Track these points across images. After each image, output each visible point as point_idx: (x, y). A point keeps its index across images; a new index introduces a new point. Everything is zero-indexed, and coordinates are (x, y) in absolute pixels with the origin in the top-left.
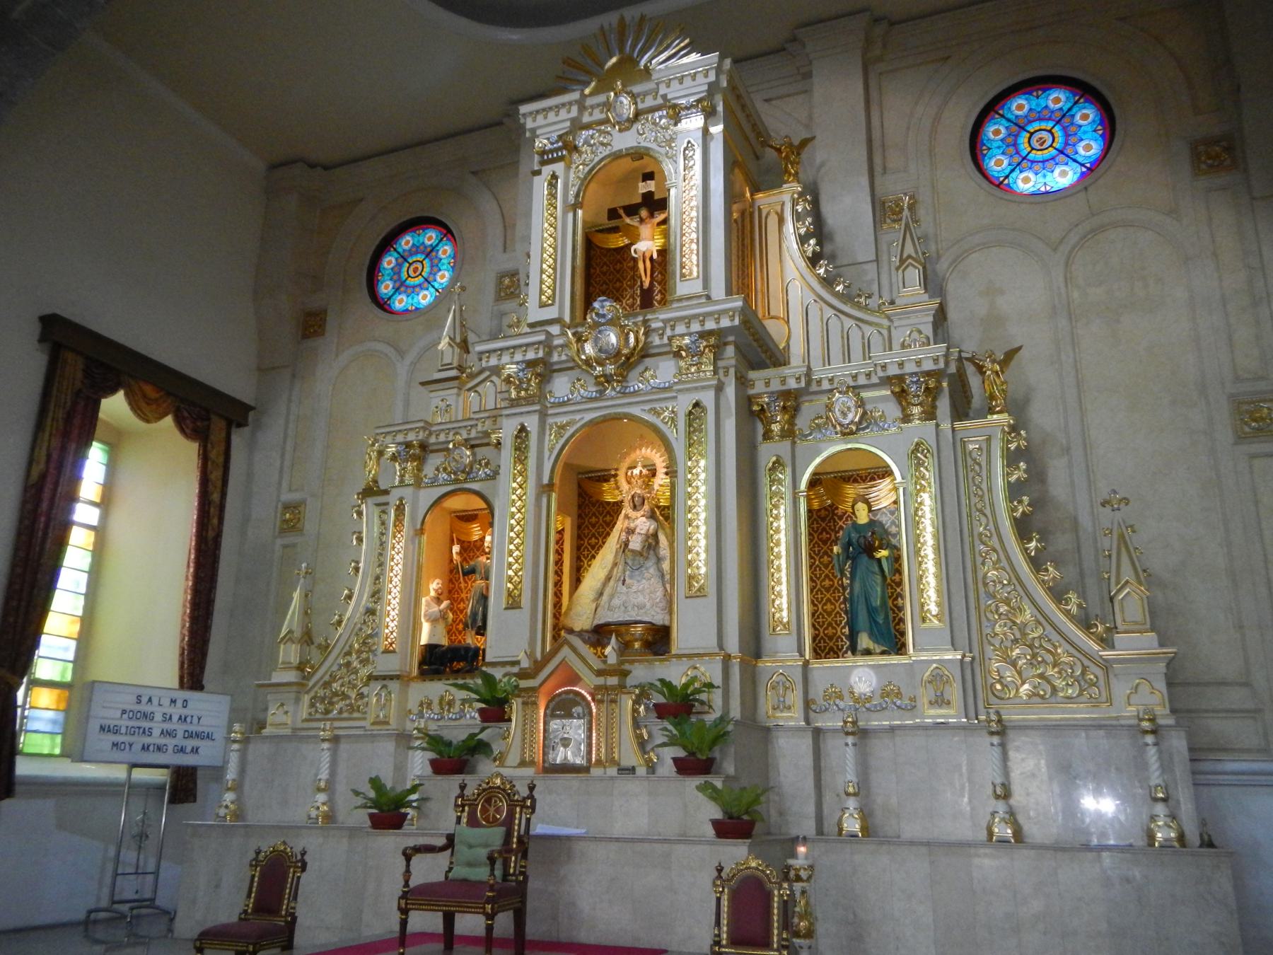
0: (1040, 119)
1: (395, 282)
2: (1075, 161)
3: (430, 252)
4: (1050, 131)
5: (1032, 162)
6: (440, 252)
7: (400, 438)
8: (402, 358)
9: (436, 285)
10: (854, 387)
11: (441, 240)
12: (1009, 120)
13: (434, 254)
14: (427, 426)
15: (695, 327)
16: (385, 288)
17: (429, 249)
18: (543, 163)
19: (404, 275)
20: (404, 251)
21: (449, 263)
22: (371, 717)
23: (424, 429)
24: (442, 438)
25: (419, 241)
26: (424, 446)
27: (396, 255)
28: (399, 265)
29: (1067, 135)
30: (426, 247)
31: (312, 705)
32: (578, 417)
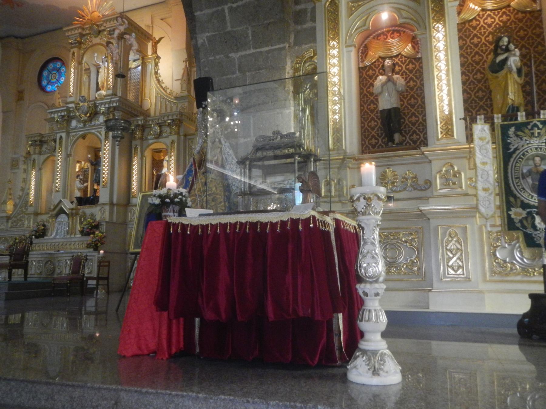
3: (58, 70)
7: (33, 139)
9: (61, 82)
10: (158, 124)
14: (41, 135)
15: (107, 106)
16: (44, 83)
18: (72, 48)
19: (50, 78)
22: (26, 226)
23: (39, 136)
24: (46, 139)
26: (41, 141)
27: (47, 70)
28: (49, 75)
31: (12, 223)
32: (78, 133)
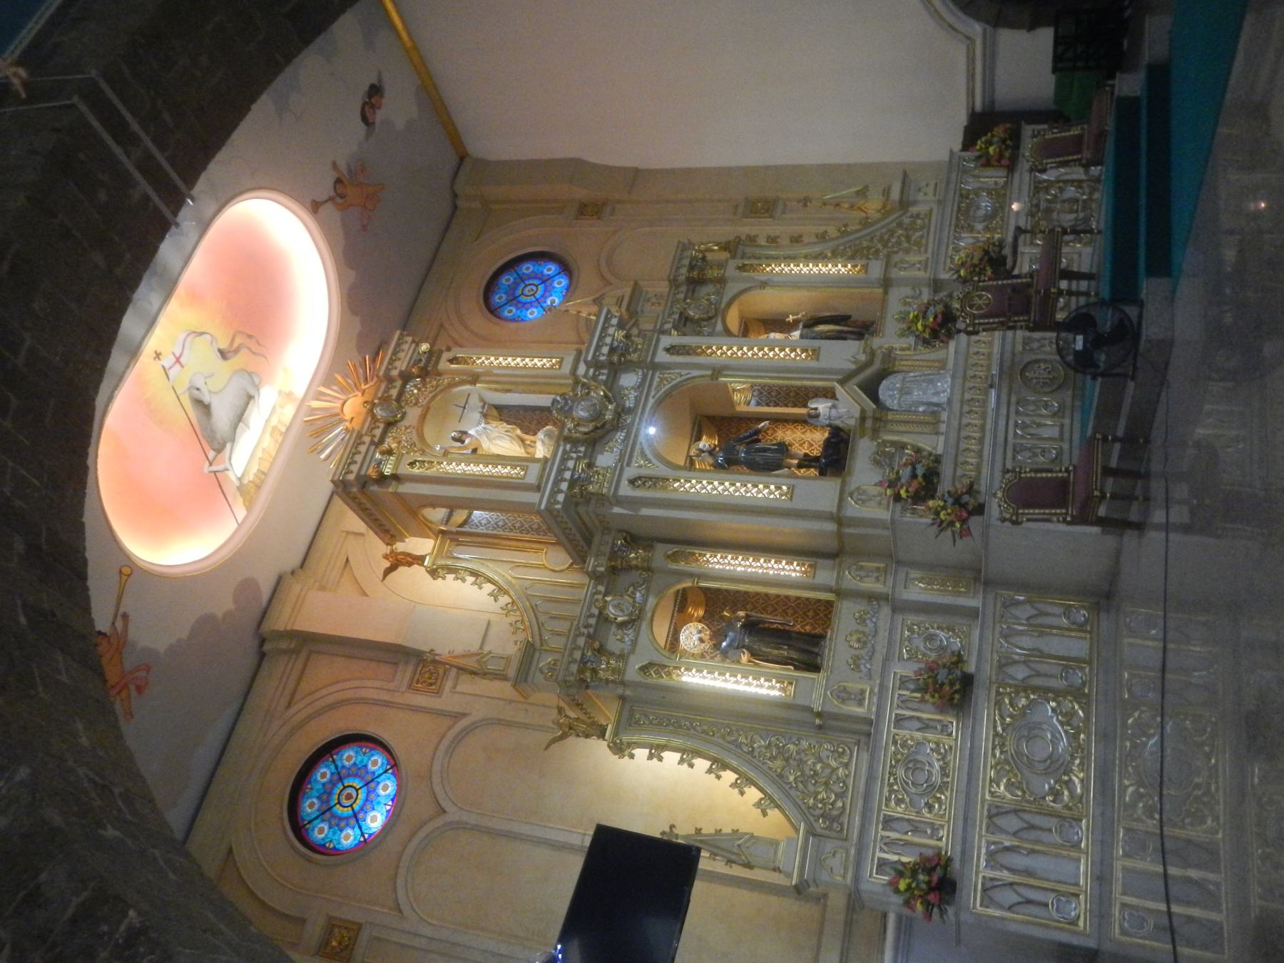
0: (515, 289)
1: (347, 825)
2: (553, 277)
4: (526, 286)
5: (542, 296)
6: (346, 764)
8: (444, 811)
9: (381, 771)
11: (334, 761)
12: (506, 304)
13: (344, 772)
16: (349, 838)
17: (335, 777)
19: (348, 812)
20: (318, 810)
21: (364, 754)
25: (318, 791)
29: (535, 278)
30: (330, 781)
